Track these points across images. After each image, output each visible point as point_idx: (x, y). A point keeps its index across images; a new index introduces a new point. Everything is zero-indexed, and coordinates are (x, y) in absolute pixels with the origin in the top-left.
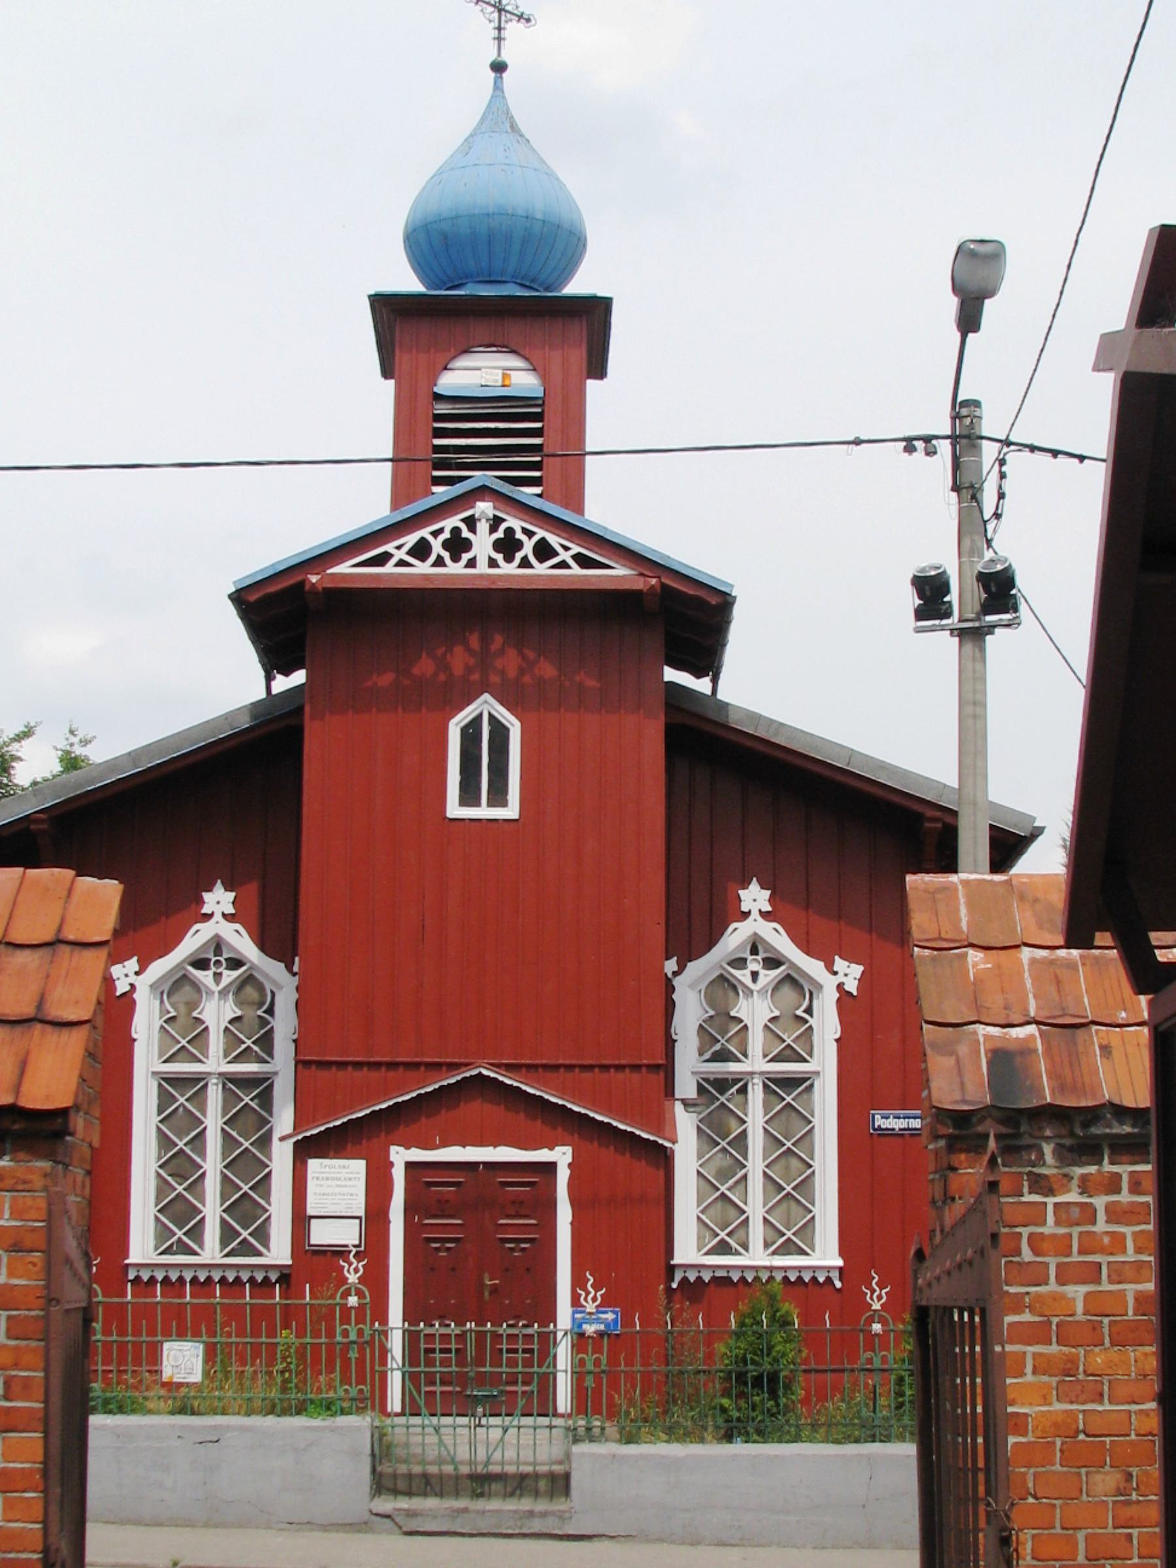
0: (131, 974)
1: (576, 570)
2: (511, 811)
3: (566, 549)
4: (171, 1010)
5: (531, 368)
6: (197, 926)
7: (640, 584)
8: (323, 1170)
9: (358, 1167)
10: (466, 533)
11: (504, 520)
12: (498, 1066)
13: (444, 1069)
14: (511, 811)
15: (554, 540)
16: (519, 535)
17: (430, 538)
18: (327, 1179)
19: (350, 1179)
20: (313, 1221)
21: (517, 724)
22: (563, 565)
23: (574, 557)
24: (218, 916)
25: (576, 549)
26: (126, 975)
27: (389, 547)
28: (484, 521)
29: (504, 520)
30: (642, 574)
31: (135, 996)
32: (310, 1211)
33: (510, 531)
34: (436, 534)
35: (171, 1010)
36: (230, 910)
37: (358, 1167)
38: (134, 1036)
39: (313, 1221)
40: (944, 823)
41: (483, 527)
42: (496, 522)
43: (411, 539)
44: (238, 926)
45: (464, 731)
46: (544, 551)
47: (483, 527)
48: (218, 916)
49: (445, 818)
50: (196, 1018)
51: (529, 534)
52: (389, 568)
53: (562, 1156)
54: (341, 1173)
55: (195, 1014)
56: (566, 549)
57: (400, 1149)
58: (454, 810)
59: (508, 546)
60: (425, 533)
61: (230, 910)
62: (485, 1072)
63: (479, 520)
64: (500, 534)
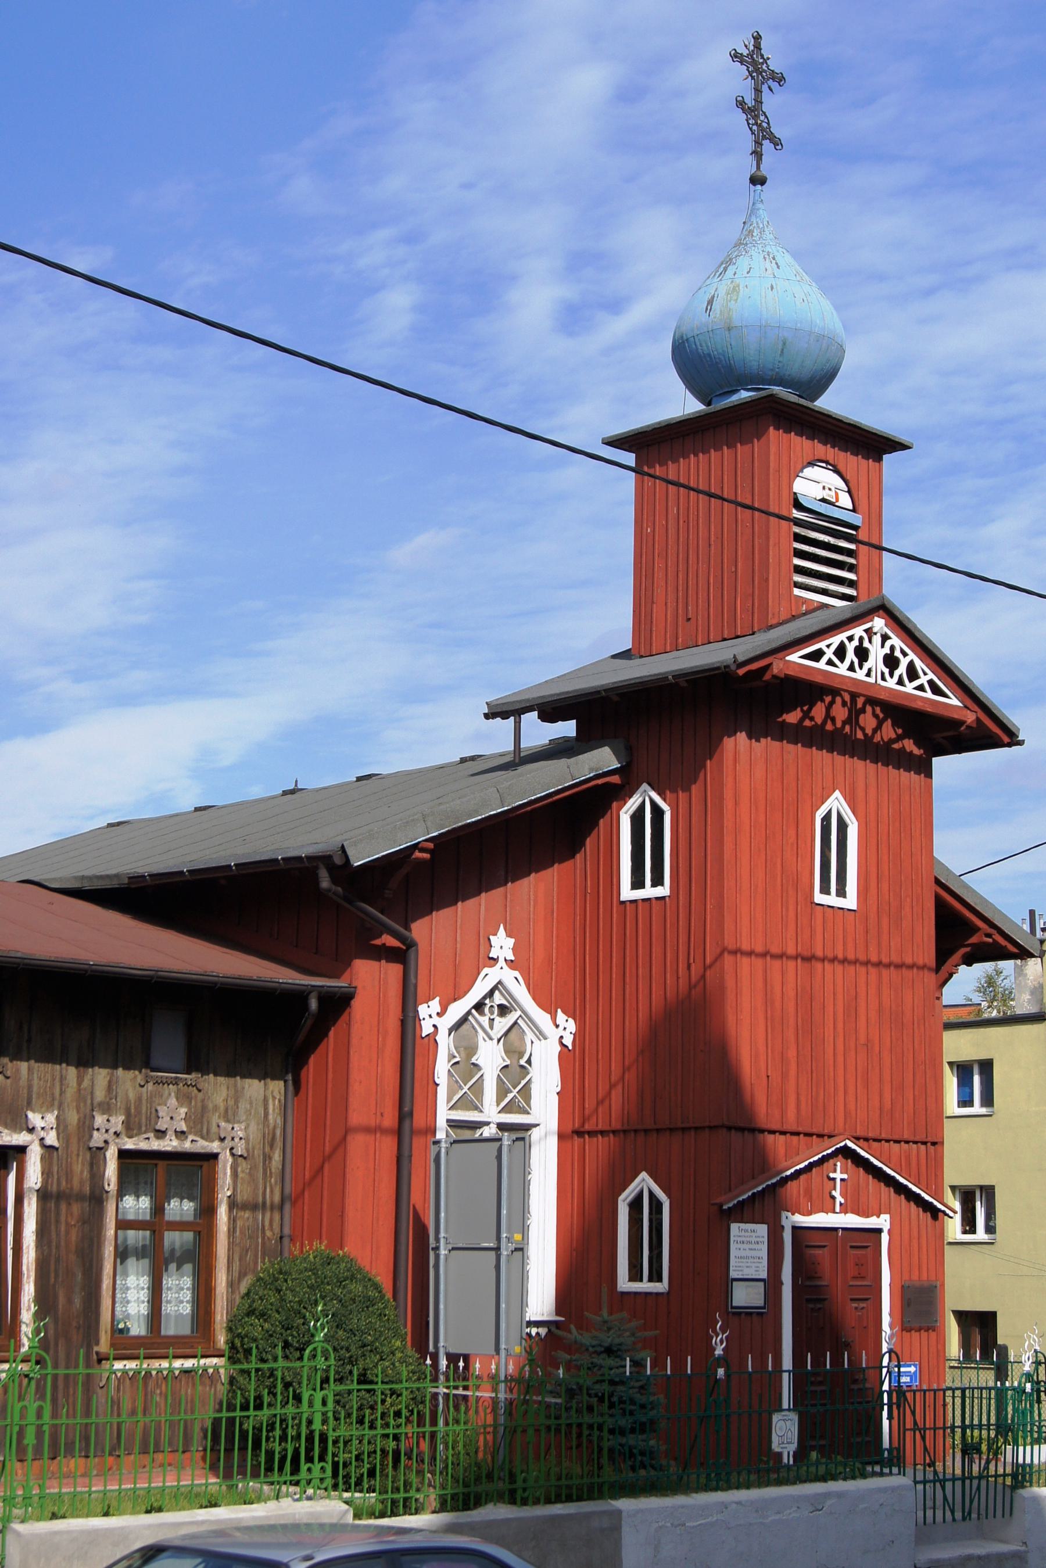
0: (434, 1015)
1: (929, 694)
2: (851, 901)
3: (925, 674)
4: (456, 1054)
5: (846, 489)
6: (486, 970)
7: (970, 718)
8: (741, 1234)
9: (762, 1229)
10: (866, 644)
11: (890, 638)
12: (858, 1138)
13: (826, 1138)
14: (851, 901)
15: (919, 664)
16: (898, 653)
17: (846, 642)
18: (743, 1243)
19: (758, 1243)
20: (734, 1283)
21: (856, 824)
22: (921, 688)
23: (931, 683)
24: (501, 963)
25: (931, 676)
26: (430, 1016)
27: (822, 645)
28: (879, 635)
29: (890, 638)
30: (966, 707)
31: (437, 1038)
32: (733, 1274)
33: (892, 648)
34: (850, 639)
35: (456, 1054)
36: (511, 956)
37: (762, 1229)
38: (437, 1081)
39: (734, 1283)
40: (993, 939)
41: (877, 639)
42: (885, 638)
43: (836, 640)
44: (517, 974)
45: (823, 820)
46: (912, 673)
47: (877, 639)
48: (501, 963)
49: (812, 903)
50: (473, 1064)
51: (905, 654)
52: (822, 665)
53: (883, 1221)
54: (752, 1236)
55: (473, 1060)
56: (925, 674)
57: (789, 1214)
58: (819, 898)
59: (891, 662)
60: (842, 637)
61: (511, 956)
62: (850, 1144)
63: (875, 634)
64: (887, 650)
